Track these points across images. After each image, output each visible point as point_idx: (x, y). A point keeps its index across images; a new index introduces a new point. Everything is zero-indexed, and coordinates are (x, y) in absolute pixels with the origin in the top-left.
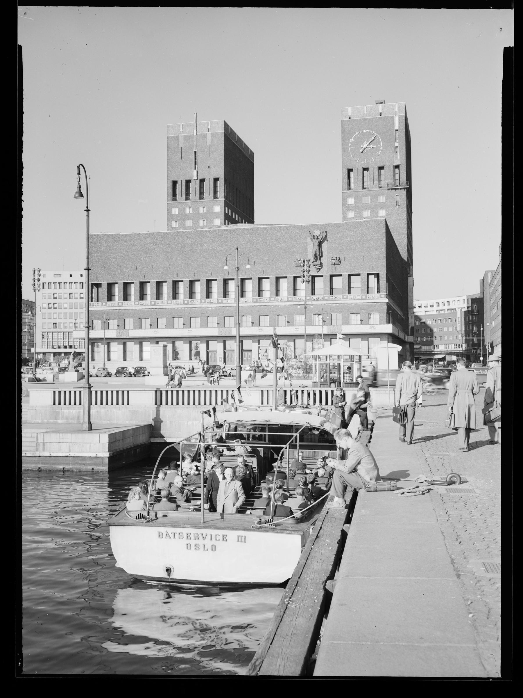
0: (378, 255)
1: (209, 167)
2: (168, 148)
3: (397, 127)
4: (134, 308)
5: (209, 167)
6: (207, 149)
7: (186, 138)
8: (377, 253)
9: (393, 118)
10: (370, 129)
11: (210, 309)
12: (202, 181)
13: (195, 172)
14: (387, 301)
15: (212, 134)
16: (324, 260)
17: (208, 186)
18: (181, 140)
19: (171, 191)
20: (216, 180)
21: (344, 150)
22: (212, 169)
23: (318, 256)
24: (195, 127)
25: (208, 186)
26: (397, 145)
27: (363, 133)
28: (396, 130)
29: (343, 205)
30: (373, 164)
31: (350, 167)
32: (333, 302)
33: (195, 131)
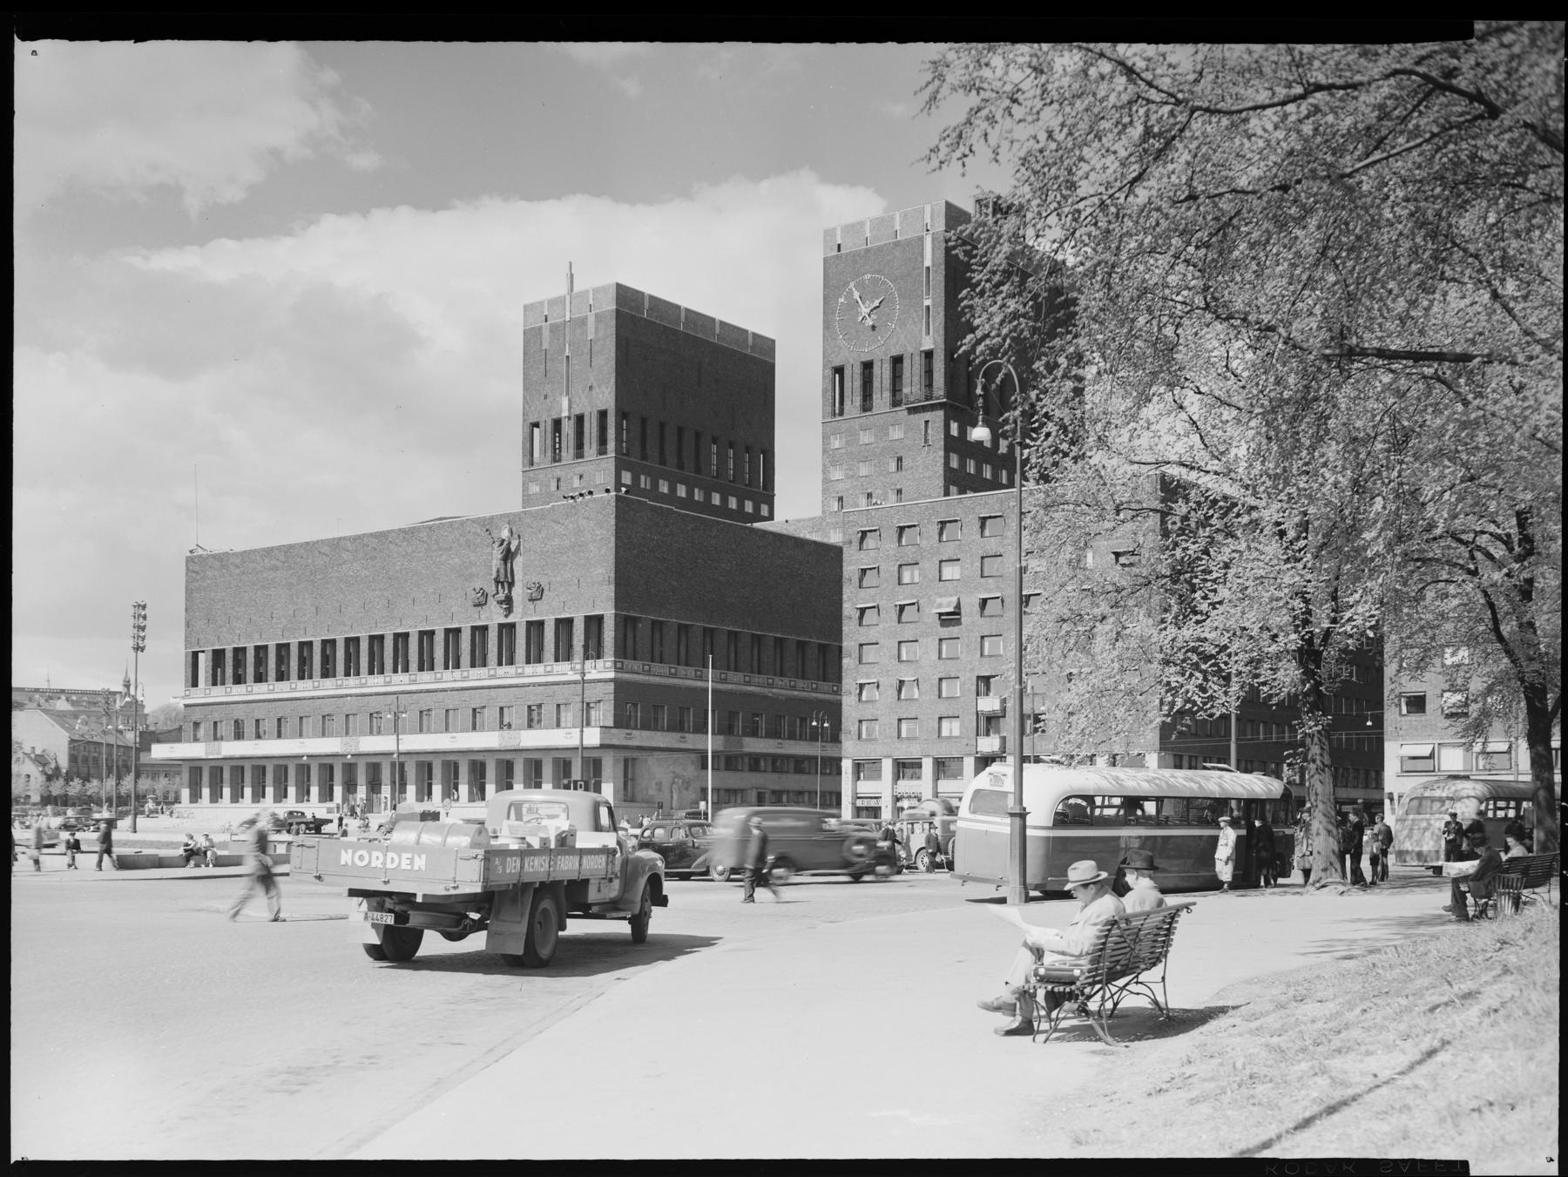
3: (928, 262)
5: (591, 388)
6: (587, 350)
7: (555, 329)
9: (921, 239)
10: (879, 272)
13: (565, 402)
15: (597, 315)
17: (591, 428)
18: (546, 333)
20: (603, 415)
21: (827, 325)
22: (596, 390)
23: (506, 581)
25: (591, 428)
29: (824, 451)
30: (879, 351)
31: (837, 363)
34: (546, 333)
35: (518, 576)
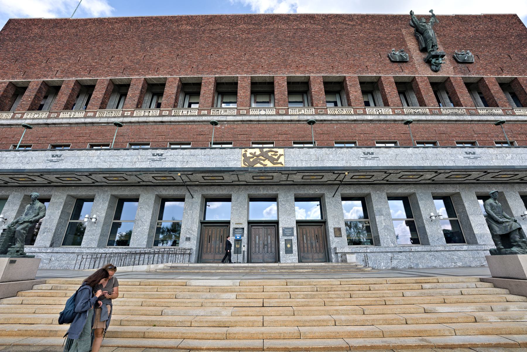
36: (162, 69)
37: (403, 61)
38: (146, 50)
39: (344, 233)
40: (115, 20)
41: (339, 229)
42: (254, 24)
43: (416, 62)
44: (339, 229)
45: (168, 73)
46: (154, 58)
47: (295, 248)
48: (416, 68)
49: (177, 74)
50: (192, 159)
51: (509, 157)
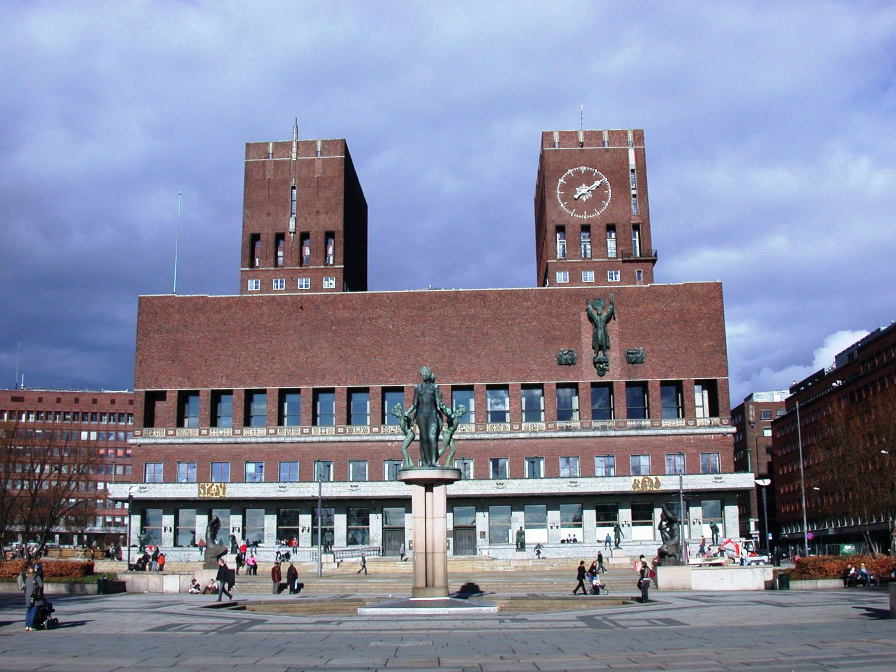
0: (713, 346)
1: (318, 212)
2: (246, 179)
4: (231, 440)
8: (711, 343)
11: (390, 444)
12: (305, 236)
14: (734, 430)
16: (614, 355)
19: (248, 250)
24: (294, 149)
26: (634, 192)
27: (580, 171)
28: (633, 171)
31: (560, 222)
32: (633, 432)
33: (294, 155)
34: (270, 167)
35: (614, 341)
36: (327, 377)
37: (571, 363)
38: (307, 350)
39: (487, 535)
40: (261, 301)
41: (484, 533)
42: (418, 309)
43: (584, 362)
44: (484, 533)
45: (335, 382)
46: (317, 361)
47: (451, 546)
48: (582, 371)
49: (345, 383)
50: (379, 489)
51: (601, 484)
